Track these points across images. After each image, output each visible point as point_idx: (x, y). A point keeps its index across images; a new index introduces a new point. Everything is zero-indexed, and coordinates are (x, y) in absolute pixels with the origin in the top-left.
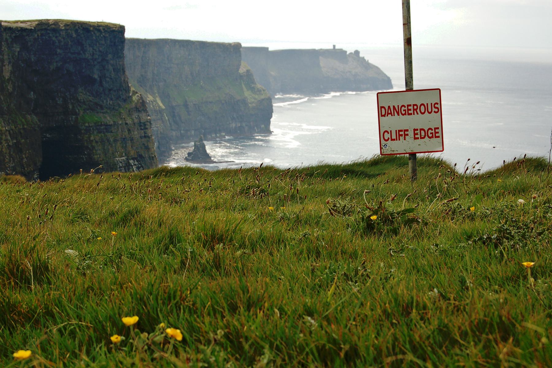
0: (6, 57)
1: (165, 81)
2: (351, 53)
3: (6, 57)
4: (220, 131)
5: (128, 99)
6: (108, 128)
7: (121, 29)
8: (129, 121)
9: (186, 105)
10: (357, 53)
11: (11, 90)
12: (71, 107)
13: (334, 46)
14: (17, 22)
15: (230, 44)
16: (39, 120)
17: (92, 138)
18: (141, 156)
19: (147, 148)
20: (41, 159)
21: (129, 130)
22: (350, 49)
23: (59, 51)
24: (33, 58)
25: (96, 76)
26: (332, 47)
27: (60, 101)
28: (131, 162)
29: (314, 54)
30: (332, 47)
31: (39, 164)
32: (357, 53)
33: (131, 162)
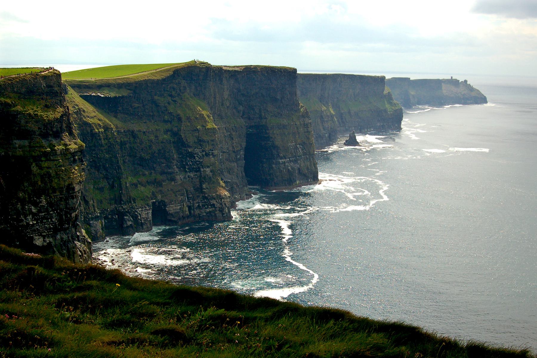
0: (226, 87)
1: (338, 98)
3: (226, 87)
4: (370, 128)
5: (298, 110)
6: (284, 127)
7: (295, 70)
8: (298, 123)
9: (349, 112)
10: (466, 81)
11: (228, 105)
12: (263, 114)
14: (234, 67)
15: (378, 77)
16: (245, 122)
17: (275, 132)
18: (304, 143)
19: (308, 138)
20: (245, 144)
21: (297, 128)
22: (461, 79)
23: (257, 83)
24: (241, 88)
25: (278, 97)
27: (257, 111)
28: (298, 146)
29: (438, 83)
31: (244, 146)
32: (466, 81)
33: (298, 146)
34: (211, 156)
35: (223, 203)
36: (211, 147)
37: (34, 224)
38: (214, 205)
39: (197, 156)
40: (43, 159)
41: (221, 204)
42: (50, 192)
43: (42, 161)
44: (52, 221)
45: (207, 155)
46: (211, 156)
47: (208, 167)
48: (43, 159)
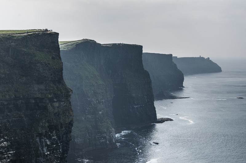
2: (206, 59)
10: (209, 58)
13: (200, 56)
15: (168, 55)
22: (206, 57)
26: (199, 57)
30: (199, 57)
32: (209, 58)
34: (101, 104)
35: (111, 136)
36: (101, 97)
37: (48, 154)
38: (105, 137)
39: (93, 104)
40: (55, 100)
41: (110, 136)
42: (59, 127)
43: (54, 102)
44: (59, 151)
45: (99, 103)
46: (101, 104)
47: (101, 111)
48: (55, 100)
